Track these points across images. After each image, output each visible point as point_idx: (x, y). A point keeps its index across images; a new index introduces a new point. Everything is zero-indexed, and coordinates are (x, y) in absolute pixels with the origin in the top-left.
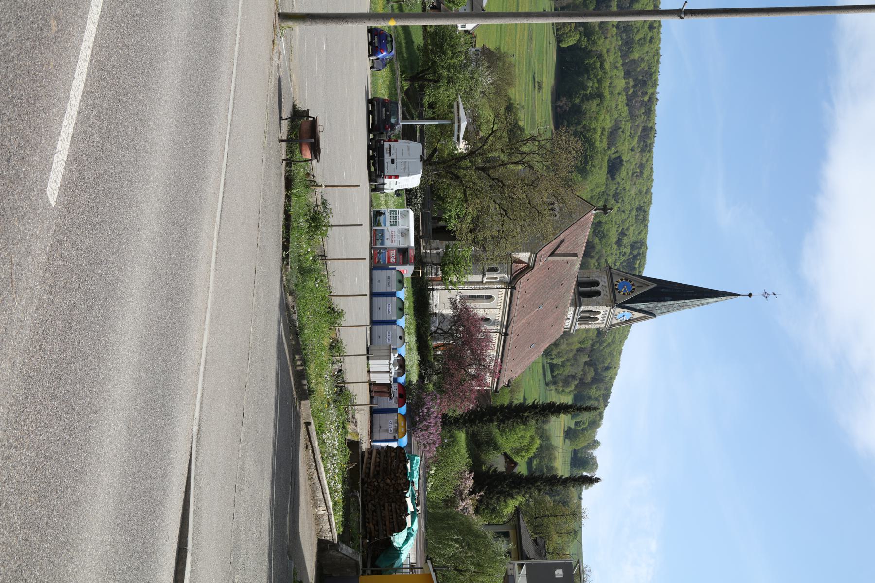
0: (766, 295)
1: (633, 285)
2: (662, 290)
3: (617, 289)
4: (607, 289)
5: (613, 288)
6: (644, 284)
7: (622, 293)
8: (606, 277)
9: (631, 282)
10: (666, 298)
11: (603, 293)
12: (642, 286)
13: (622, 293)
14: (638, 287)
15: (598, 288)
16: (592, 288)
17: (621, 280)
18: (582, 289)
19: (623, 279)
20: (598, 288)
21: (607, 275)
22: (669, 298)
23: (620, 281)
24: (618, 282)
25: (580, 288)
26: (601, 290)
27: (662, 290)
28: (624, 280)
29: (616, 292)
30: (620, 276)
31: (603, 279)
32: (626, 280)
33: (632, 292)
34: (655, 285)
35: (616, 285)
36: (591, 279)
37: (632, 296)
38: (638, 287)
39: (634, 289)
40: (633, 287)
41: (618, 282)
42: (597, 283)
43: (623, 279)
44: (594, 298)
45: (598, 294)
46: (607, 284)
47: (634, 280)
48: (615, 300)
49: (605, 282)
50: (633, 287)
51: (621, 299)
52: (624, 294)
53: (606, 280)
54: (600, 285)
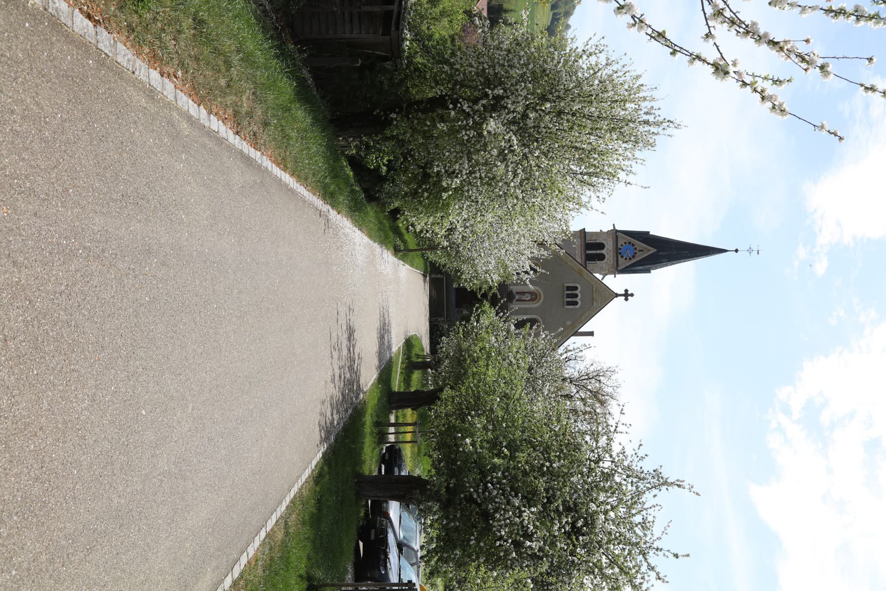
0: (750, 251)
2: (661, 253)
3: (620, 253)
4: (611, 254)
5: (618, 252)
7: (624, 258)
8: (611, 240)
10: (663, 260)
11: (607, 257)
12: (642, 251)
13: (624, 258)
14: (639, 251)
15: (603, 252)
16: (598, 252)
17: (625, 243)
18: (588, 252)
20: (603, 252)
22: (665, 260)
24: (622, 245)
26: (606, 254)
27: (661, 253)
28: (627, 244)
29: (619, 256)
33: (634, 257)
34: (655, 250)
35: (620, 249)
36: (598, 241)
37: (633, 261)
38: (639, 251)
41: (622, 245)
42: (601, 246)
45: (601, 257)
46: (611, 248)
48: (618, 265)
49: (610, 246)
51: (623, 263)
52: (626, 259)
53: (611, 244)
54: (605, 249)
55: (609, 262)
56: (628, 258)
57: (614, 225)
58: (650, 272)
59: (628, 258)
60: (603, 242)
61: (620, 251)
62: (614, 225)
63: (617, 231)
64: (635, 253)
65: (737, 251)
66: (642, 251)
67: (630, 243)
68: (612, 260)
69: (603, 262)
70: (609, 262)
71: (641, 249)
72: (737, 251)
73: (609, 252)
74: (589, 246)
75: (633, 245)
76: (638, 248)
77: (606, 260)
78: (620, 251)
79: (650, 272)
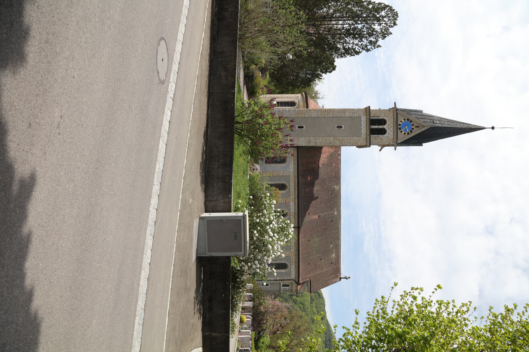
1: (413, 125)
4: (392, 129)
5: (398, 127)
6: (420, 124)
7: (403, 133)
9: (411, 122)
11: (388, 131)
12: (418, 127)
13: (403, 133)
14: (416, 127)
15: (385, 127)
16: (381, 127)
17: (404, 120)
19: (406, 119)
20: (385, 127)
21: (393, 115)
23: (403, 121)
24: (401, 122)
25: (371, 126)
26: (387, 129)
28: (406, 120)
29: (399, 131)
30: (404, 116)
31: (390, 118)
32: (408, 120)
33: (411, 132)
35: (400, 125)
36: (380, 118)
38: (416, 127)
39: (413, 129)
40: (413, 127)
41: (401, 122)
42: (383, 122)
43: (406, 119)
44: (380, 136)
45: (383, 132)
47: (414, 122)
48: (397, 139)
50: (413, 127)
51: (402, 137)
52: (405, 134)
53: (392, 120)
55: (390, 136)
56: (406, 133)
57: (395, 103)
58: (422, 145)
59: (406, 133)
60: (385, 118)
61: (400, 127)
62: (395, 103)
63: (397, 110)
64: (413, 129)
65: (493, 128)
66: (418, 127)
67: (408, 120)
68: (392, 135)
69: (385, 135)
70: (390, 136)
71: (417, 125)
72: (493, 128)
73: (390, 127)
74: (373, 122)
75: (411, 122)
76: (415, 125)
77: (387, 134)
78: (400, 127)
79: (422, 145)
